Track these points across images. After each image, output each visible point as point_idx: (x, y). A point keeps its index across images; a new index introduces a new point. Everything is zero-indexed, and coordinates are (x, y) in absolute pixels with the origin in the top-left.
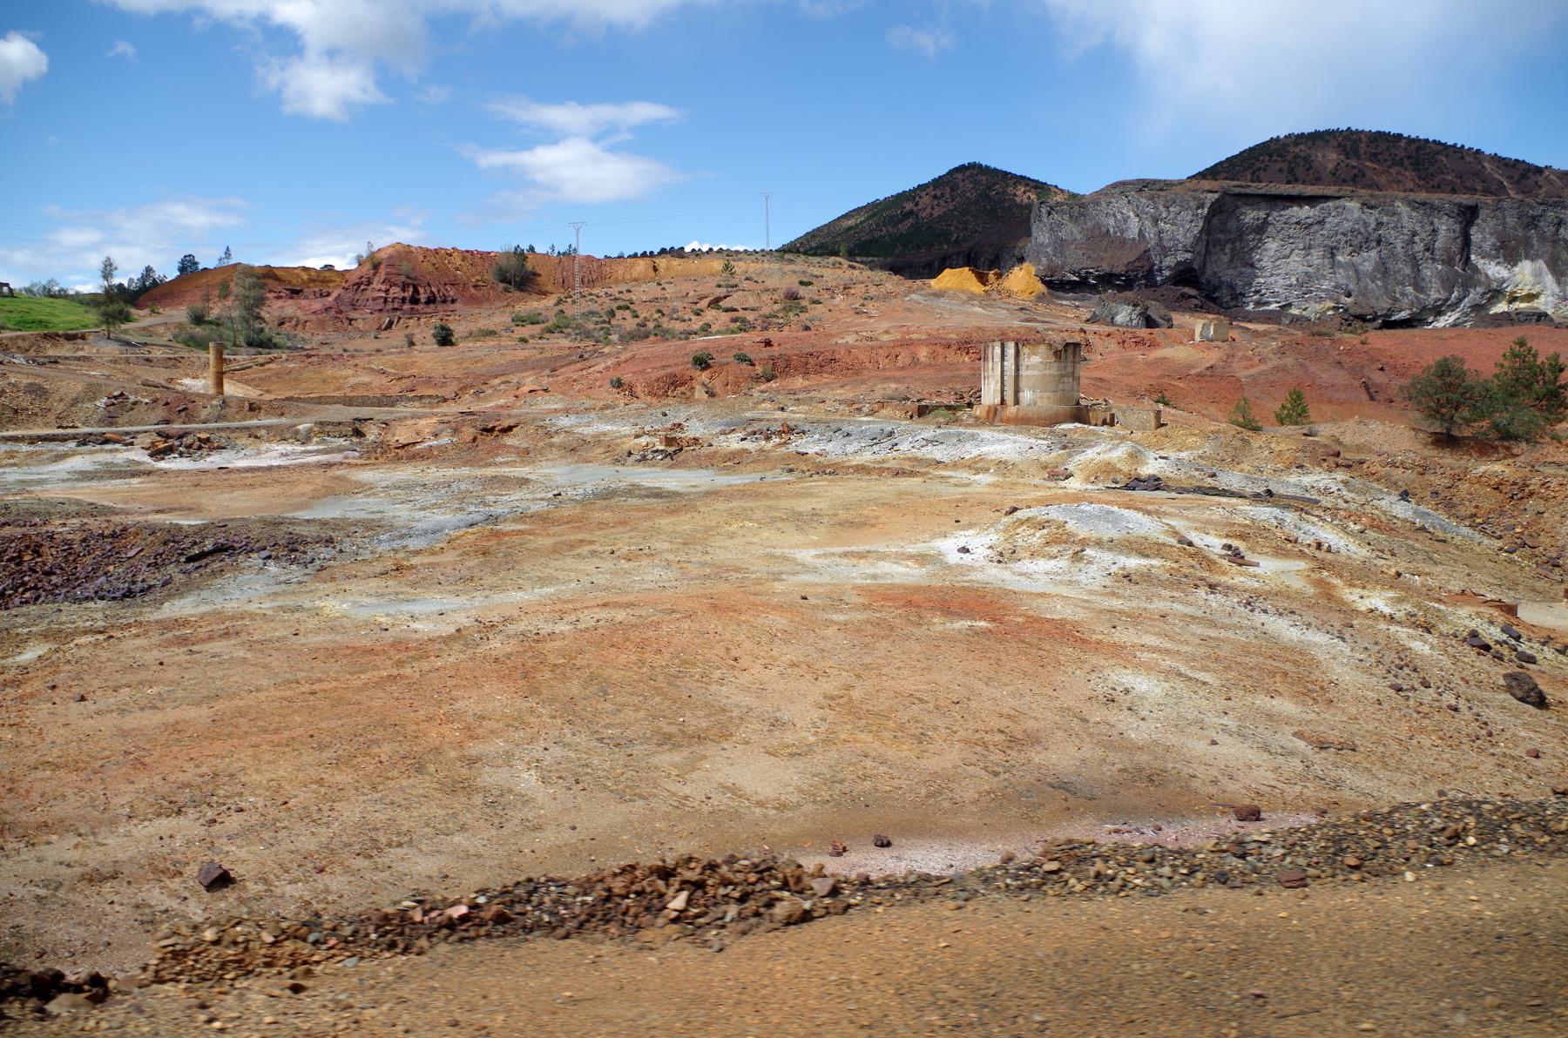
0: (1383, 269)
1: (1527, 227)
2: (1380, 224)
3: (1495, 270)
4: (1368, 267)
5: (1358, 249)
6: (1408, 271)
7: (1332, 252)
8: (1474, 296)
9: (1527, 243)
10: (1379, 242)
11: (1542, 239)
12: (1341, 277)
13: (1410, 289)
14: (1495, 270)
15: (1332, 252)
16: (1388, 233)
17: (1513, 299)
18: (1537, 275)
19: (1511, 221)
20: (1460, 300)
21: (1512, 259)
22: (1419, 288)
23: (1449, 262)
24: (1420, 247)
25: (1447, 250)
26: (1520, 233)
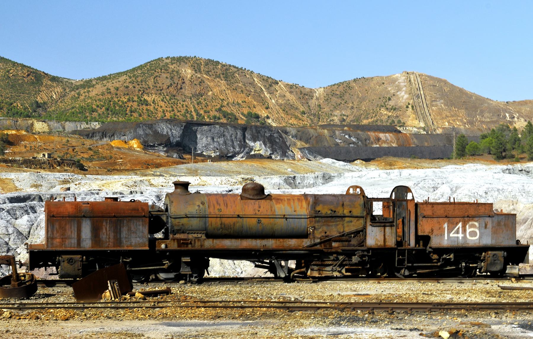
0: (225, 143)
1: (258, 133)
2: (224, 132)
3: (252, 144)
4: (222, 142)
5: (219, 137)
6: (231, 143)
7: (213, 139)
8: (247, 150)
9: (258, 138)
10: (224, 136)
11: (261, 136)
12: (216, 145)
13: (232, 148)
14: (252, 144)
15: (213, 139)
16: (226, 134)
17: (255, 151)
18: (261, 145)
19: (254, 131)
20: (243, 151)
21: (255, 141)
22: (234, 148)
23: (240, 141)
24: (233, 137)
25: (239, 138)
26: (256, 134)
